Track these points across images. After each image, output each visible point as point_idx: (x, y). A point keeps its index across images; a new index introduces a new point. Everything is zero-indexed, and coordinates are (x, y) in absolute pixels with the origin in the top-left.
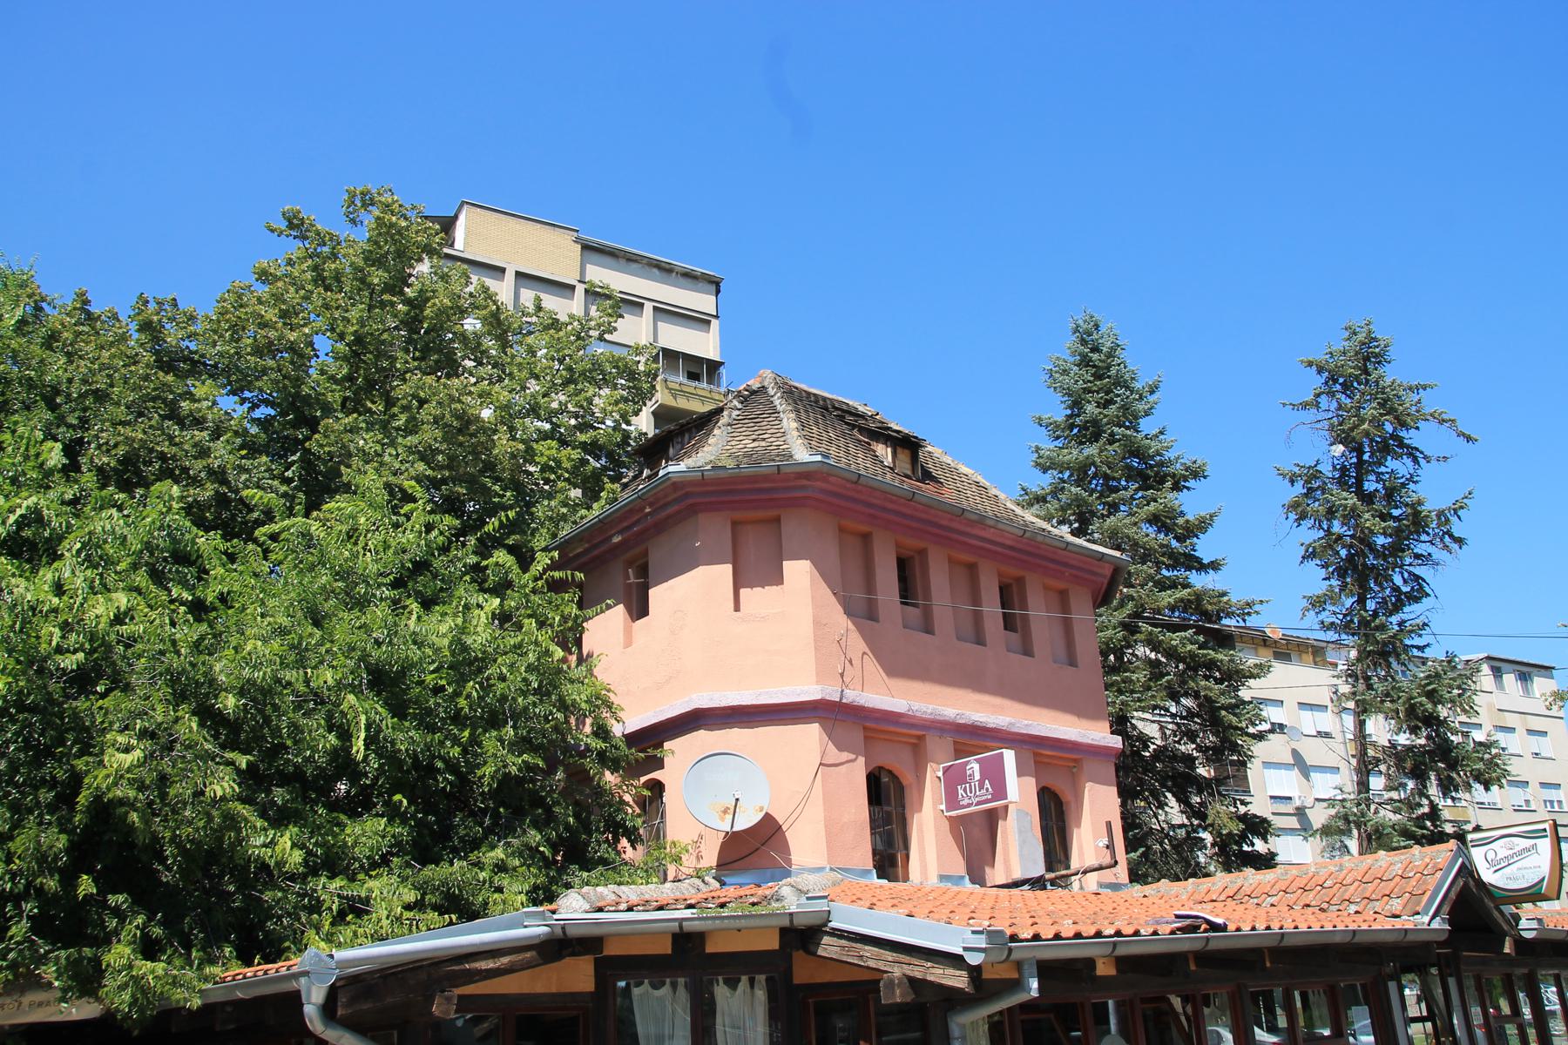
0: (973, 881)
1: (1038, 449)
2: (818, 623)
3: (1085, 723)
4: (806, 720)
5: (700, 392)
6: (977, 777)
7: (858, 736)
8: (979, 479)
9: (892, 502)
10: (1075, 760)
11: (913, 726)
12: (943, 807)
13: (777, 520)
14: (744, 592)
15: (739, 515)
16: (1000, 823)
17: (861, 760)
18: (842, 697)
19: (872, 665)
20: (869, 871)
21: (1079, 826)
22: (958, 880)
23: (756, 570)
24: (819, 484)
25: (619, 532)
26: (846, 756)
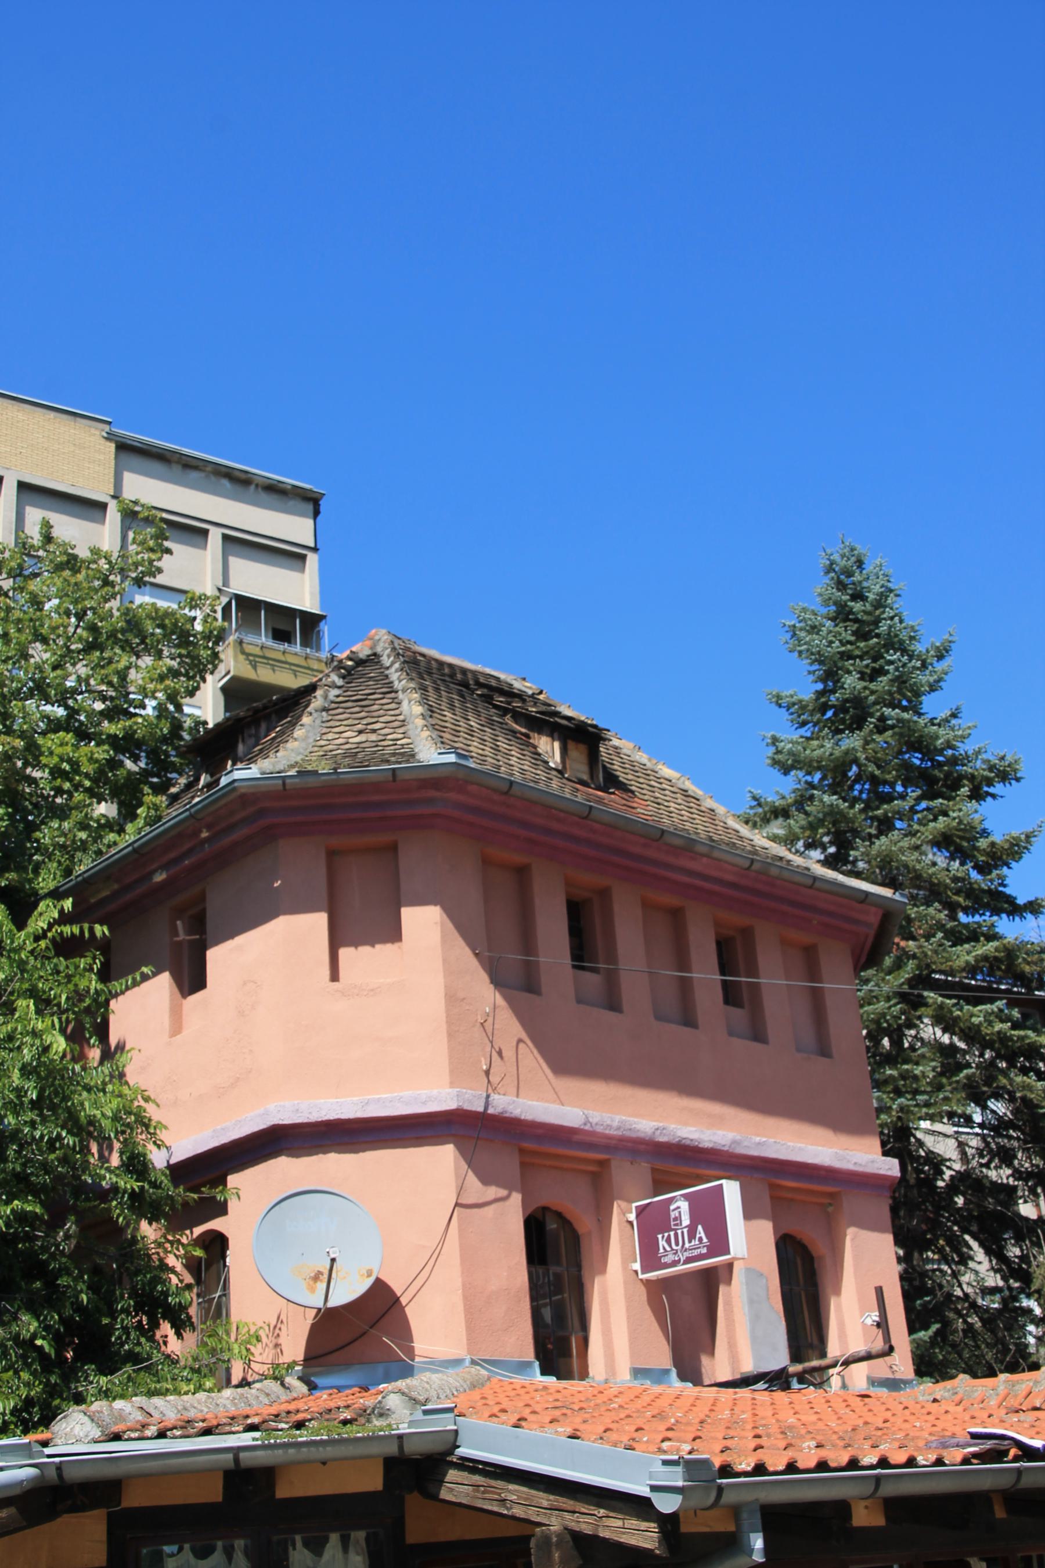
0: (683, 1377)
1: (775, 740)
2: (452, 998)
5: (291, 659)
6: (686, 1221)
7: (511, 1164)
8: (688, 785)
10: (831, 1195)
11: (591, 1146)
12: (637, 1266)
13: (393, 848)
16: (722, 1289)
17: (517, 1198)
18: (487, 1105)
19: (531, 1059)
20: (528, 1365)
21: (838, 1292)
22: (660, 1376)
23: (361, 920)
24: (453, 796)
25: (164, 867)
26: (493, 1192)
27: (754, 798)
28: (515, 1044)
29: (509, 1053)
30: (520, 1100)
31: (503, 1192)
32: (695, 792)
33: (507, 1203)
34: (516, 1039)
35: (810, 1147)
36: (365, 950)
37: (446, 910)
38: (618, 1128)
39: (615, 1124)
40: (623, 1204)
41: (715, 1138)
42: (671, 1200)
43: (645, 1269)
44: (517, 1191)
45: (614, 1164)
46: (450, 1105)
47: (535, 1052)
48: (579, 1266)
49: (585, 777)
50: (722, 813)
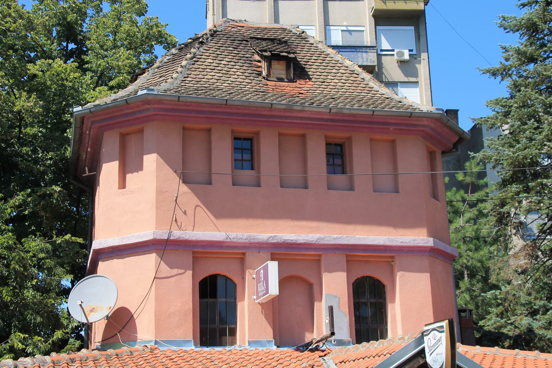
2: (159, 192)
3: (401, 231)
4: (149, 252)
7: (189, 258)
9: (217, 107)
10: (393, 257)
12: (255, 297)
13: (141, 131)
14: (129, 176)
15: (123, 130)
16: (316, 304)
17: (189, 273)
19: (203, 213)
21: (393, 301)
24: (155, 106)
26: (175, 271)
27: (504, 48)
28: (194, 208)
29: (190, 212)
30: (194, 232)
31: (183, 271)
32: (358, 71)
33: (184, 275)
34: (195, 205)
35: (371, 237)
36: (135, 174)
37: (158, 154)
38: (246, 239)
39: (244, 237)
40: (251, 271)
41: (307, 238)
42: (260, 270)
43: (258, 298)
44: (190, 270)
45: (247, 253)
46: (150, 237)
47: (206, 210)
48: (235, 298)
49: (284, 76)
50: (367, 79)
